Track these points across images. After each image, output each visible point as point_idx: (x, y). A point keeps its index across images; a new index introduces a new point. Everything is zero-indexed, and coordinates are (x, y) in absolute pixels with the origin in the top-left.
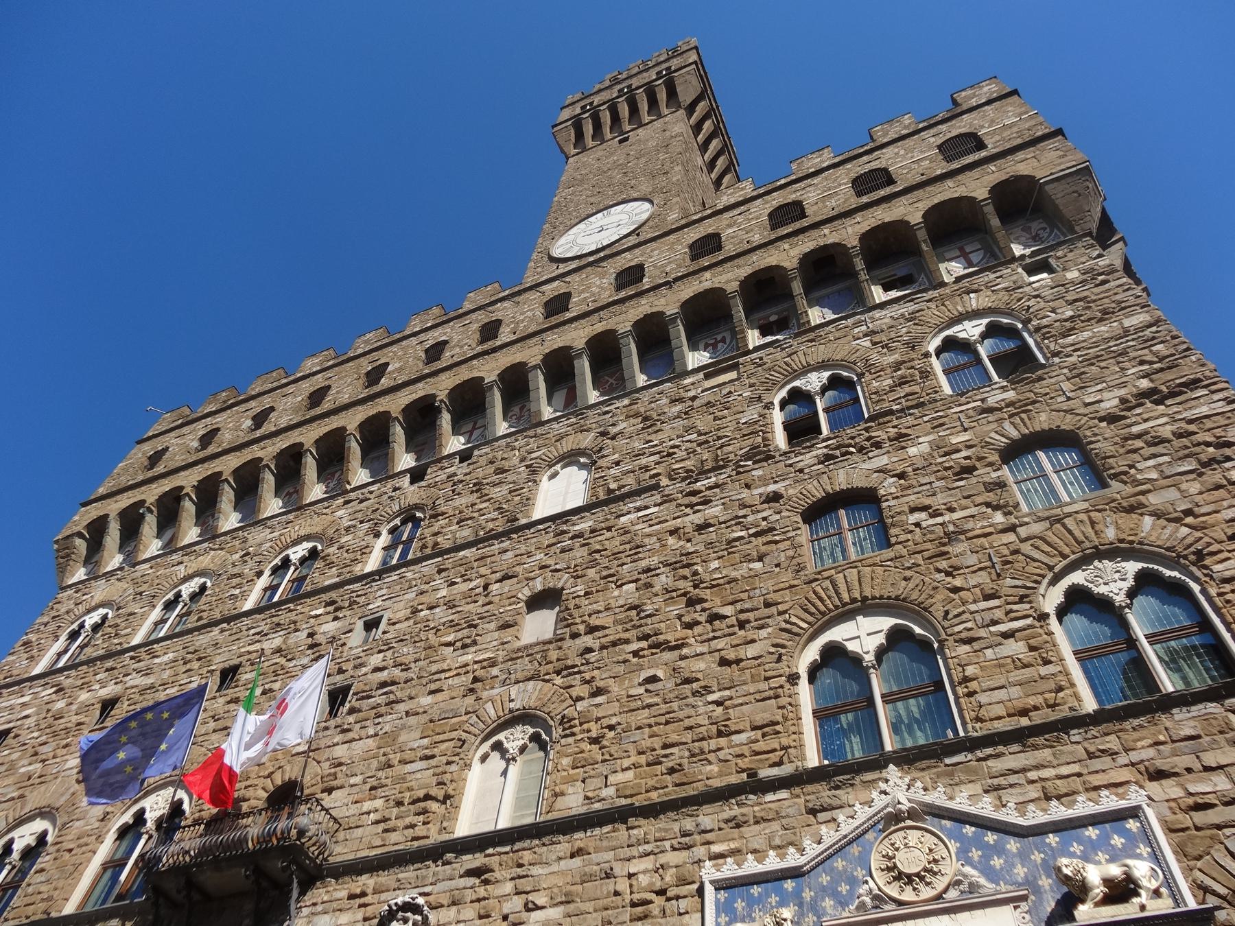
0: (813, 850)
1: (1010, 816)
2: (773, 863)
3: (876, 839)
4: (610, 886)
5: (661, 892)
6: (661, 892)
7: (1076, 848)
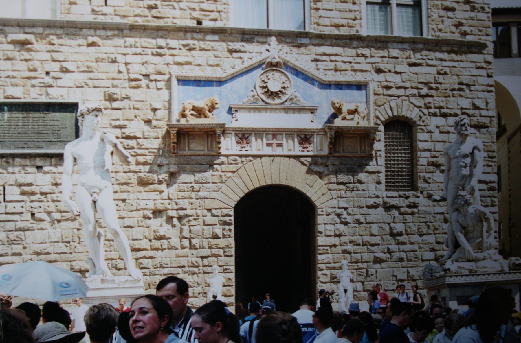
0: (230, 72)
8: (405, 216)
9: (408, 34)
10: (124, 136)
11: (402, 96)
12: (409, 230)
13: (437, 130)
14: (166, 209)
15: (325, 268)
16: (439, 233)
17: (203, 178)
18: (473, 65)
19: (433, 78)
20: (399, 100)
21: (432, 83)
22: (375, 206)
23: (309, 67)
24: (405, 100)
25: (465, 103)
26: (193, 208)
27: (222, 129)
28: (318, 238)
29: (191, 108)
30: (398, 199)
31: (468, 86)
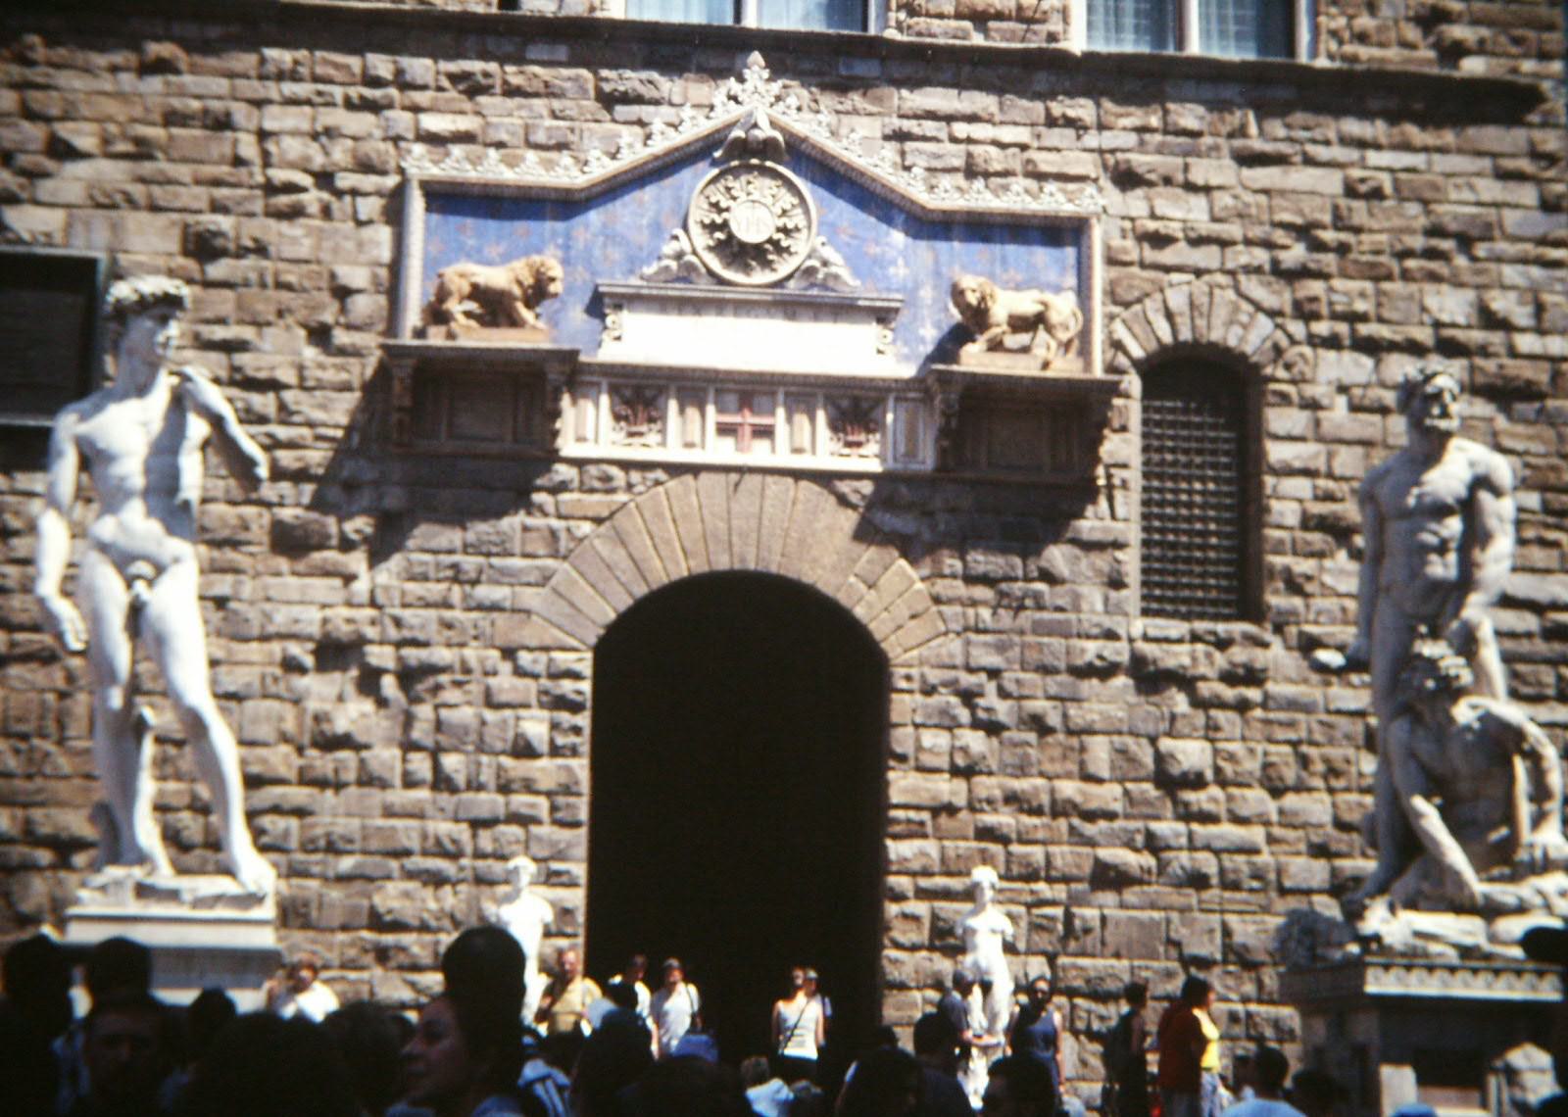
0: (601, 168)
1: (915, 188)
2: (532, 171)
4: (222, 144)
5: (324, 178)
6: (324, 178)
8: (1213, 712)
9: (1235, 53)
10: (238, 377)
11: (1208, 271)
12: (1228, 769)
13: (1341, 401)
14: (361, 641)
15: (911, 894)
16: (1348, 790)
17: (494, 538)
18: (1486, 163)
19: (1328, 206)
20: (1200, 286)
21: (1324, 227)
22: (1105, 671)
23: (878, 162)
24: (1221, 287)
26: (455, 640)
27: (567, 369)
28: (891, 775)
29: (466, 289)
30: (1185, 648)
31: (1465, 242)
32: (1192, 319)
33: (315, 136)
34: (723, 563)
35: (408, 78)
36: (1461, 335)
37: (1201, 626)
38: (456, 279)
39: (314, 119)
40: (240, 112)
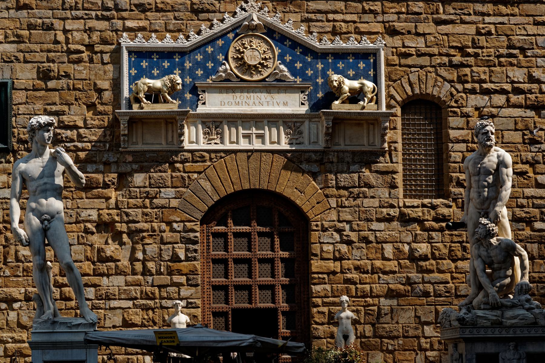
0: (195, 39)
2: (169, 42)
3: (234, 38)
4: (50, 35)
5: (90, 47)
7: (341, 65)
11: (426, 66)
20: (422, 72)
21: (469, 47)
24: (430, 72)
25: (518, 74)
31: (523, 50)
32: (420, 85)
33: (85, 31)
34: (247, 186)
35: (120, 7)
36: (521, 86)
37: (426, 201)
38: (142, 85)
39: (85, 25)
40: (58, 24)
